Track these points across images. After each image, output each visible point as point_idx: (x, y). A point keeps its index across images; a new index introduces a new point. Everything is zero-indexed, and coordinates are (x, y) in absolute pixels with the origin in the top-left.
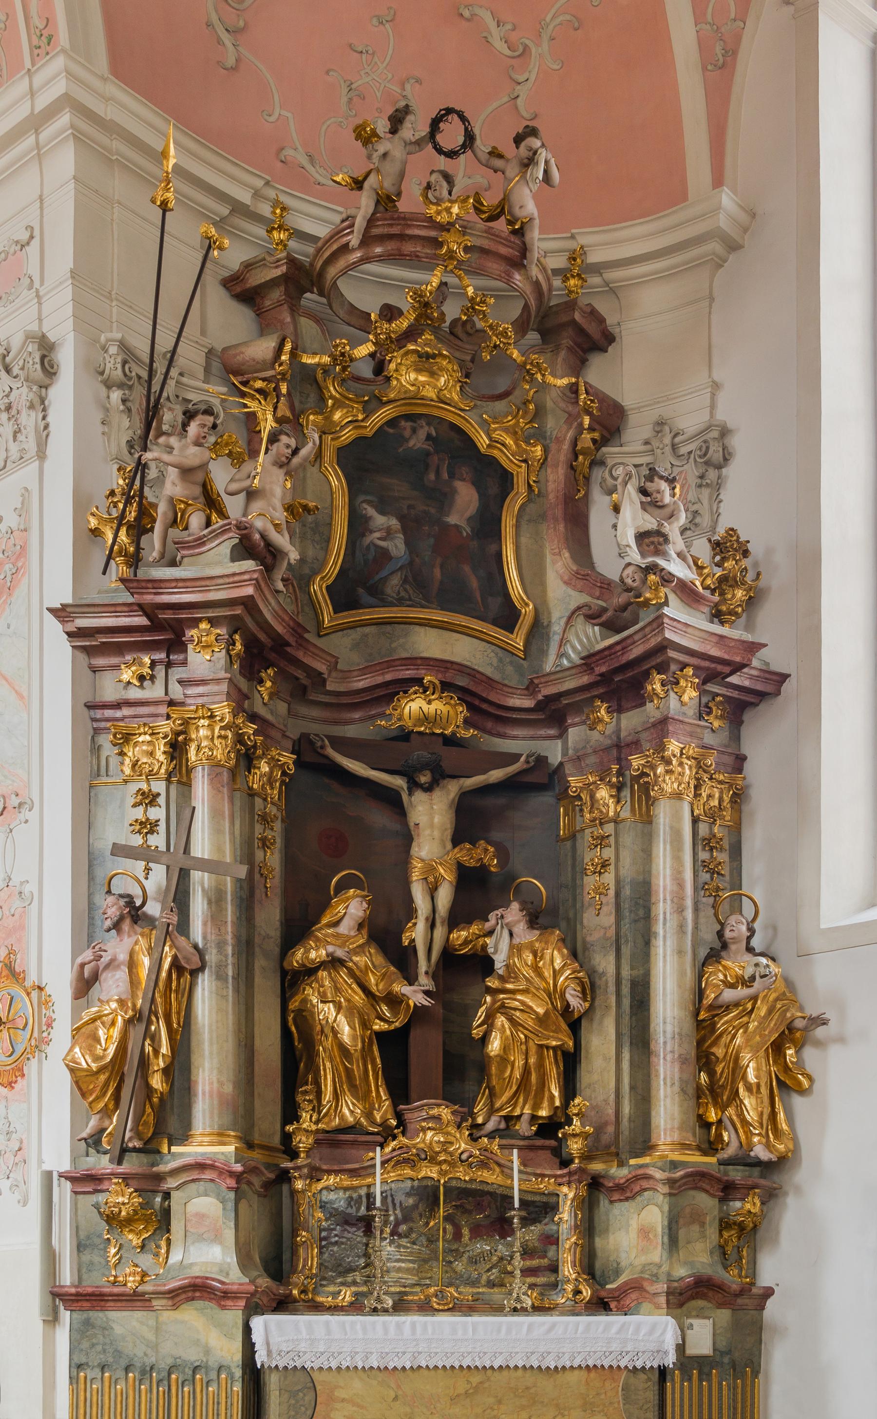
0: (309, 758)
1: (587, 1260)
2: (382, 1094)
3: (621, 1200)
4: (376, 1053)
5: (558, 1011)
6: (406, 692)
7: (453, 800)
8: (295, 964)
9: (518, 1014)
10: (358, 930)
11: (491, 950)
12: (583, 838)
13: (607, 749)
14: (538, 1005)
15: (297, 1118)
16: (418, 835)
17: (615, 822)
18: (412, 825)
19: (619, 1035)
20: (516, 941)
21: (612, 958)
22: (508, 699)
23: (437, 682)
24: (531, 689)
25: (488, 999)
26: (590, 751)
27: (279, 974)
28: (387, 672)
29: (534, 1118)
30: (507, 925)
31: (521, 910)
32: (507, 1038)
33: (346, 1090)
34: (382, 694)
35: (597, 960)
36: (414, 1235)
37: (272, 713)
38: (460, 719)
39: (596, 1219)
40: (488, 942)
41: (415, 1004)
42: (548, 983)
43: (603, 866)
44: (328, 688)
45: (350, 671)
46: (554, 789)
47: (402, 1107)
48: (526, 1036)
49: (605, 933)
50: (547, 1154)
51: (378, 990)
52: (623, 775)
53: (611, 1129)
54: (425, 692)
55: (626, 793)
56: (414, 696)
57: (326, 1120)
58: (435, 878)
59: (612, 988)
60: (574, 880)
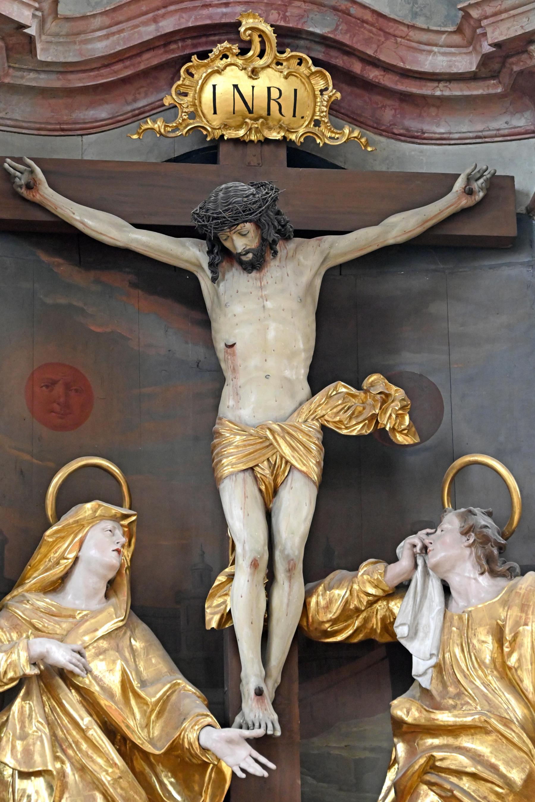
6: (203, 55)
7: (310, 285)
9: (466, 783)
10: (107, 596)
14: (510, 763)
16: (234, 370)
18: (220, 346)
22: (421, 57)
23: (268, 29)
24: (468, 31)
25: (401, 749)
28: (163, 16)
30: (435, 568)
31: (465, 533)
34: (155, 62)
38: (322, 107)
40: (396, 610)
41: (234, 774)
45: (84, 18)
51: (151, 741)
54: (244, 51)
58: (273, 467)
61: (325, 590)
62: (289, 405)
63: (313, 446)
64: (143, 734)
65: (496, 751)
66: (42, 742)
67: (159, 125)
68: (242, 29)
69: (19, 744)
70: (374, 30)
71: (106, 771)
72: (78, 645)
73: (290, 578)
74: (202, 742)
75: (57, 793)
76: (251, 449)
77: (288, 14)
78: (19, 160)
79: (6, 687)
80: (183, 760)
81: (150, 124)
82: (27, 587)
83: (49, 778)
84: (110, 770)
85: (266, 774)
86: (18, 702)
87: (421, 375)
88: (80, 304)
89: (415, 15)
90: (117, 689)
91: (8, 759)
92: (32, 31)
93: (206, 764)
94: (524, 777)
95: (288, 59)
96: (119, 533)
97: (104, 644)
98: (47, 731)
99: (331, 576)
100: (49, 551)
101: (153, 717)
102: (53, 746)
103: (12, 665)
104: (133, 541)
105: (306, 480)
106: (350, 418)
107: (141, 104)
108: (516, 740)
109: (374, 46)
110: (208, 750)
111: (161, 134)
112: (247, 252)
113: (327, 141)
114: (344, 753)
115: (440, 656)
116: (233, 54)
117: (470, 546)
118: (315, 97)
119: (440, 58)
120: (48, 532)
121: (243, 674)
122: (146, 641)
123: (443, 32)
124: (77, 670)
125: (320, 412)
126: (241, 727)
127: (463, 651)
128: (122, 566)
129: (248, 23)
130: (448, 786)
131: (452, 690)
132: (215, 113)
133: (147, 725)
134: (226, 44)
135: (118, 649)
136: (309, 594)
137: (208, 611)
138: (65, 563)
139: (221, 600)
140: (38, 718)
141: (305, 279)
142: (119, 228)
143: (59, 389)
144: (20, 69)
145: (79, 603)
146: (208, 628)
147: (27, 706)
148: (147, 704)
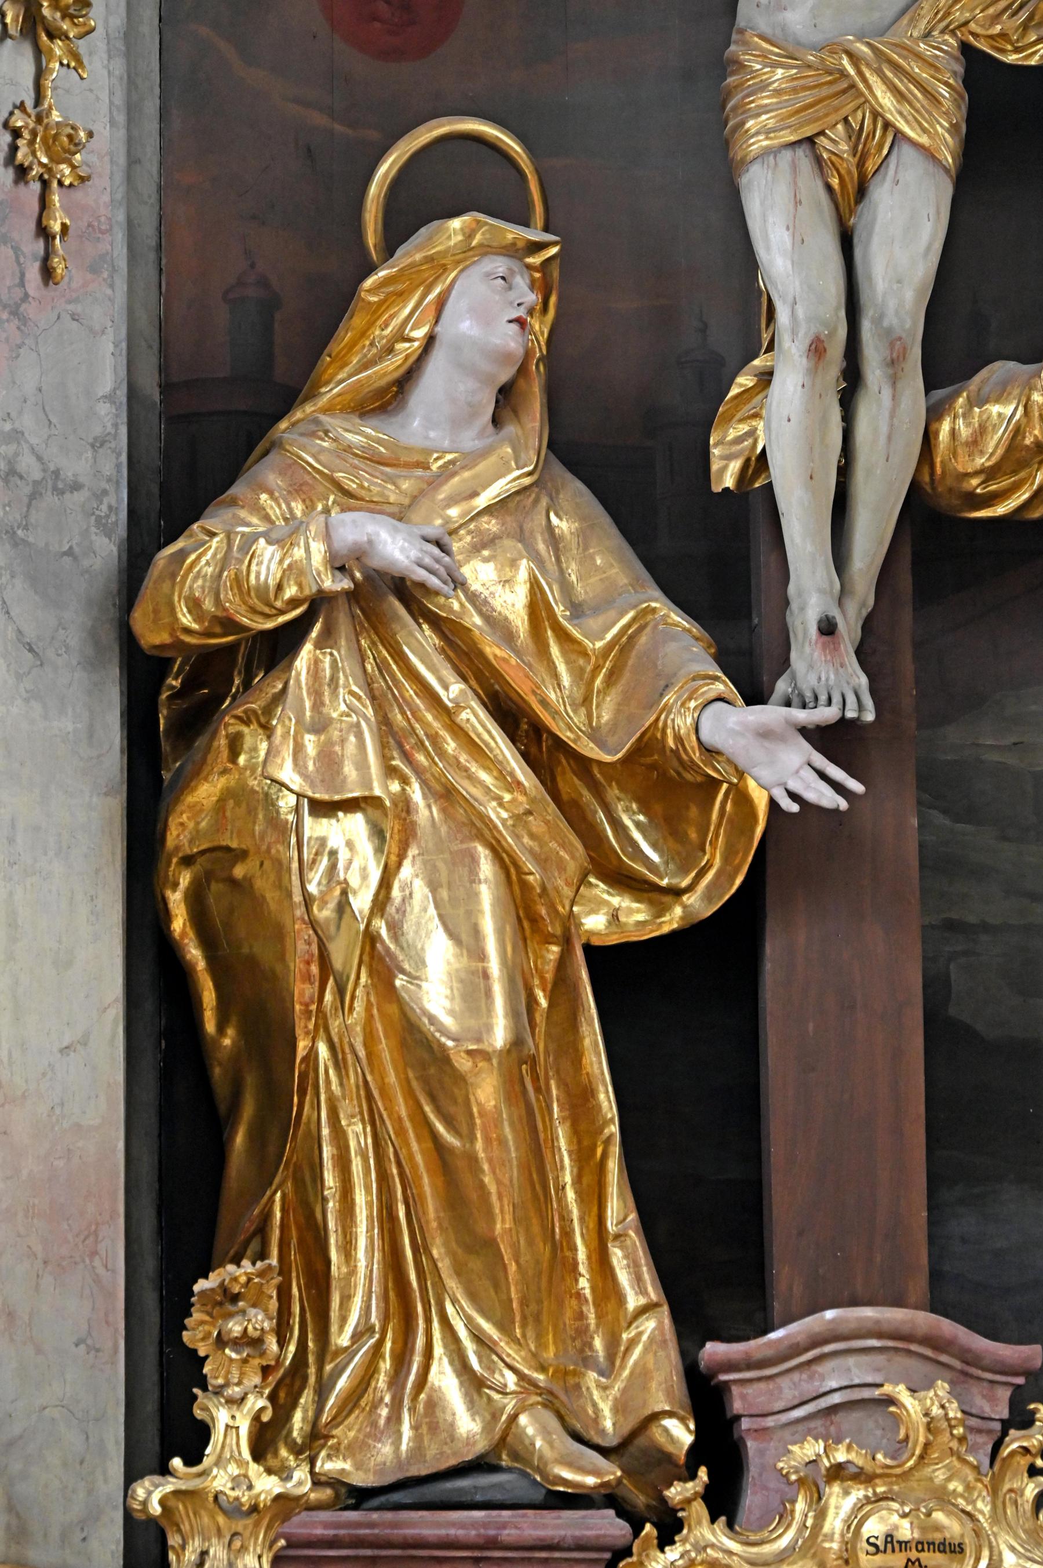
2: (623, 1277)
8: (186, 619)
10: (496, 421)
27: (114, 672)
33: (444, 1266)
41: (773, 804)
47: (714, 1350)
51: (595, 735)
57: (346, 1433)
58: (855, 136)
61: (971, 404)
63: (944, 91)
64: (579, 719)
66: (359, 735)
69: (311, 743)
71: (499, 799)
72: (435, 527)
73: (894, 381)
74: (705, 735)
75: (392, 845)
76: (807, 96)
79: (282, 619)
80: (663, 774)
82: (323, 401)
83: (375, 814)
84: (507, 797)
85: (843, 804)
86: (307, 651)
90: (519, 618)
91: (287, 773)
93: (715, 784)
96: (521, 282)
97: (491, 525)
98: (370, 712)
99: (984, 373)
100: (371, 324)
101: (598, 682)
102: (383, 747)
104: (553, 300)
105: (931, 168)
106: (1025, 27)
110: (719, 753)
114: (1011, 760)
120: (369, 283)
121: (792, 589)
122: (582, 519)
124: (434, 581)
125: (958, 15)
126: (788, 704)
128: (528, 354)
133: (586, 701)
135: (522, 536)
136: (934, 414)
137: (716, 452)
139: (743, 428)
140: (350, 684)
145: (437, 436)
146: (717, 488)
147: (328, 659)
148: (584, 653)
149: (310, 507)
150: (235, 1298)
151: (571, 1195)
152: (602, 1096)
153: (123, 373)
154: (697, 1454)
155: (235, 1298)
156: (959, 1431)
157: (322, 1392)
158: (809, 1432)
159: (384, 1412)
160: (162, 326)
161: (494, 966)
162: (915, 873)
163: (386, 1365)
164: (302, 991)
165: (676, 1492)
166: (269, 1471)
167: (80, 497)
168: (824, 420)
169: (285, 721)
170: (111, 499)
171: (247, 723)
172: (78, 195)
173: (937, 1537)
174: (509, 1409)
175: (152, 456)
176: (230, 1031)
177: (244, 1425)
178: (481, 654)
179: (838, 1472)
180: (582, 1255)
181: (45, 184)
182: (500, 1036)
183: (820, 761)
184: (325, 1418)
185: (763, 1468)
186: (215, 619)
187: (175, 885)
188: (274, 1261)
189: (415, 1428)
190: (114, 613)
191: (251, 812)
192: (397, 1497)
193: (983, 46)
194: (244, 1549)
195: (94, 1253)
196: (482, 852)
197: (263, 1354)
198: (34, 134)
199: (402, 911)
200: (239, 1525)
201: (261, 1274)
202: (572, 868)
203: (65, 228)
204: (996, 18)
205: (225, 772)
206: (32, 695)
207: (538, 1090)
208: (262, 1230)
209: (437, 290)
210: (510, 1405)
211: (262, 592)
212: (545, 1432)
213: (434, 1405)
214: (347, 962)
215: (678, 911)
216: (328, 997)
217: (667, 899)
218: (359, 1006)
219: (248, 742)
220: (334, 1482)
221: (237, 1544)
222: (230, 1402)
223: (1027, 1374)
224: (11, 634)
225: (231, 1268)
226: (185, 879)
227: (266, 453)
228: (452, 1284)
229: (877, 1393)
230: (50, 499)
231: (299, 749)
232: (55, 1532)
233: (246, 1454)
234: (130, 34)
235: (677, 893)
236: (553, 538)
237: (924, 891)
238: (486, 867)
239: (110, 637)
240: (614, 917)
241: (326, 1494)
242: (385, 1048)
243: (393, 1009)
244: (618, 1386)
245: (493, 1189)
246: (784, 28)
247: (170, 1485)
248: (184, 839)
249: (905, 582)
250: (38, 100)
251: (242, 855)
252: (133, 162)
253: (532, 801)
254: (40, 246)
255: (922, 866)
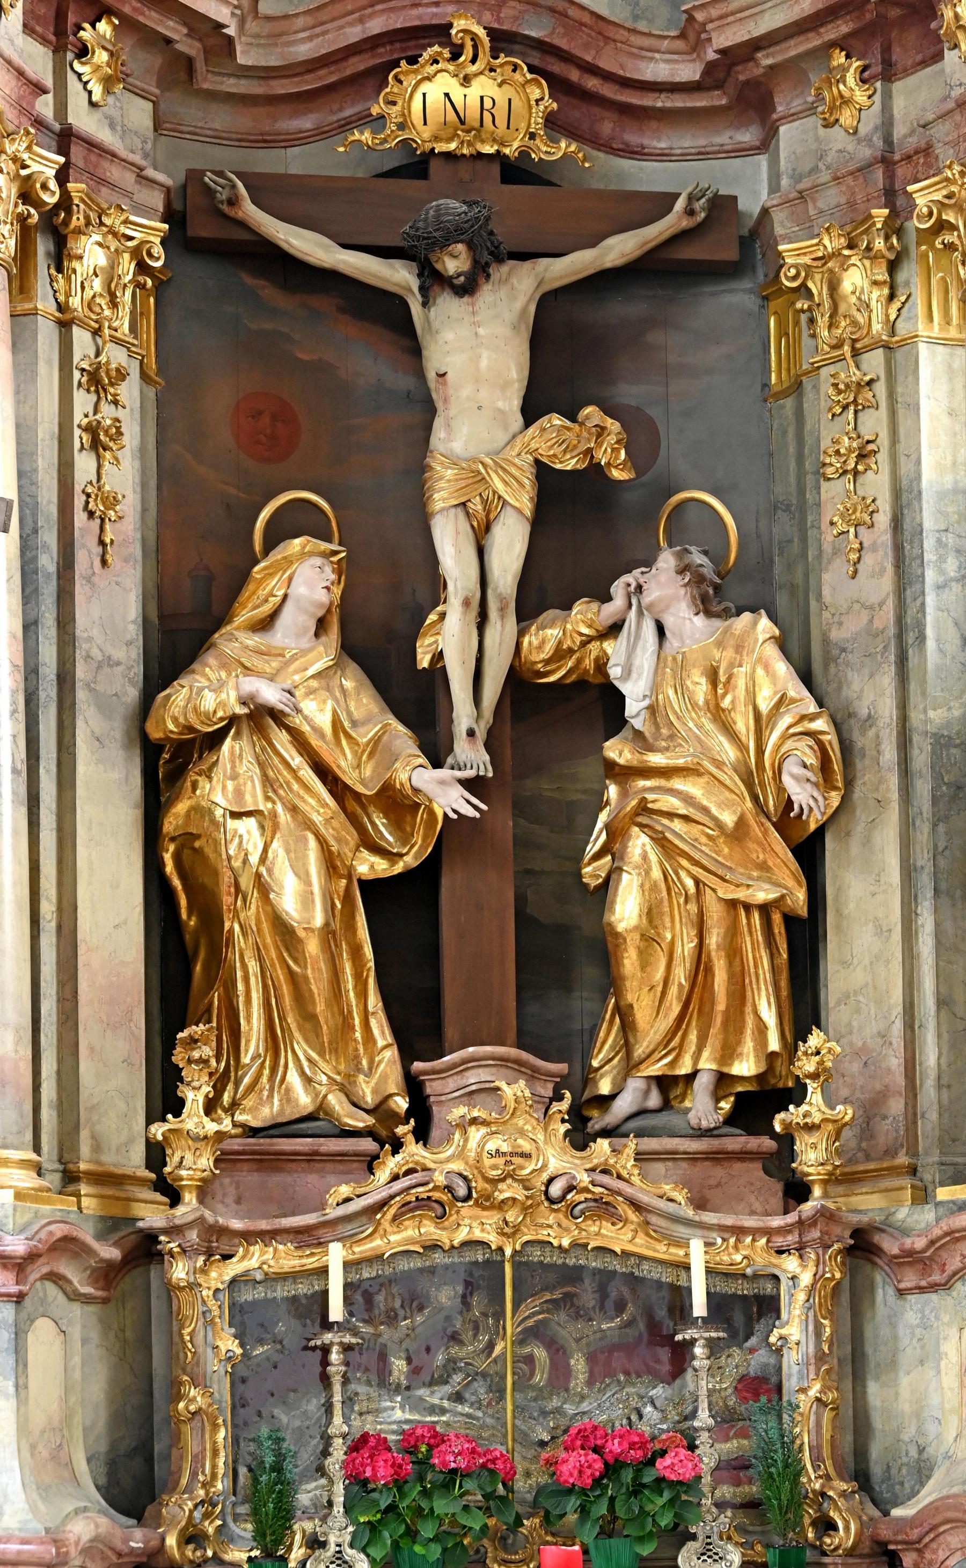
0: (201, 228)
1: (849, 1438)
2: (376, 1032)
3: (921, 1290)
4: (363, 933)
5: (769, 818)
6: (413, 60)
7: (524, 311)
8: (171, 726)
9: (677, 825)
10: (317, 635)
11: (614, 672)
12: (816, 388)
13: (863, 170)
15: (176, 1106)
16: (446, 401)
17: (887, 347)
18: (431, 375)
19: (908, 871)
20: (672, 643)
21: (887, 680)
22: (642, 65)
23: (481, 32)
24: (692, 36)
25: (613, 791)
26: (825, 177)
27: (137, 751)
28: (370, 16)
29: (723, 1080)
30: (650, 607)
31: (681, 572)
32: (654, 887)
33: (293, 1026)
34: (362, 67)
35: (856, 686)
36: (457, 1378)
37: (112, 126)
39: (868, 1333)
40: (609, 651)
41: (445, 815)
42: (741, 747)
43: (862, 456)
44: (241, 59)
45: (286, 17)
46: (754, 271)
47: (418, 1066)
48: (697, 882)
49: (871, 621)
50: (756, 1169)
51: (363, 782)
52: (900, 232)
53: (896, 1106)
54: (455, 56)
55: (910, 273)
56: (432, 69)
57: (248, 1103)
58: (485, 502)
59: (889, 754)
60: (801, 491)
61: (538, 629)
62: (502, 438)
63: (527, 481)
64: (355, 774)
65: (708, 792)
66: (253, 781)
67: (366, 137)
68: (453, 32)
69: (230, 785)
70: (593, 34)
71: (318, 812)
72: (288, 684)
73: (502, 618)
74: (414, 783)
75: (268, 833)
77: (502, 15)
78: (220, 174)
79: (216, 727)
80: (394, 801)
81: (357, 135)
82: (235, 624)
83: (261, 818)
86: (228, 742)
87: (638, 408)
88: (286, 330)
89: (636, 18)
90: (328, 729)
91: (218, 798)
92: (231, 31)
93: (419, 805)
94: (735, 819)
95: (502, 65)
96: (328, 569)
97: (314, 684)
98: (258, 771)
99: (545, 615)
100: (257, 588)
101: (364, 758)
102: (264, 786)
103: (222, 704)
104: (343, 578)
105: (520, 517)
106: (565, 451)
107: (347, 113)
108: (728, 782)
109: (593, 52)
111: (369, 147)
112: (459, 275)
113: (543, 156)
114: (556, 795)
115: (654, 698)
116: (444, 59)
117: (685, 585)
118: (530, 107)
119: (662, 66)
121: (454, 715)
122: (357, 681)
123: (666, 37)
124: (287, 710)
125: (533, 445)
126: (453, 768)
127: (676, 692)
128: (331, 603)
129: (460, 24)
130: (659, 828)
131: (664, 731)
132: (425, 124)
133: (359, 766)
134: (436, 48)
135: (328, 689)
136: (521, 633)
137: (419, 650)
138: (274, 601)
139: (432, 639)
140: (248, 757)
141: (519, 304)
142: (326, 249)
143: (266, 420)
144: (220, 74)
145: (290, 642)
146: (420, 667)
147: (237, 746)
148: (358, 744)
149: (229, 674)
150: (196, 1041)
151: (352, 994)
152: (366, 949)
153: (140, 611)
154: (410, 1113)
155: (196, 1041)
156: (530, 1102)
157: (237, 1084)
158: (461, 1103)
159: (266, 1093)
160: (159, 588)
161: (316, 889)
162: (511, 848)
163: (266, 1072)
164: (227, 900)
165: (400, 1130)
166: (213, 1120)
167: (120, 669)
168: (470, 637)
169: (218, 774)
170: (135, 670)
171: (200, 775)
172: (117, 525)
173: (520, 1150)
174: (323, 1092)
175: (156, 651)
176: (194, 918)
177: (201, 1099)
178: (309, 744)
179: (474, 1121)
180: (357, 1021)
181: (102, 520)
182: (318, 920)
183: (468, 795)
184: (238, 1096)
185: (440, 1119)
186: (185, 727)
187: (167, 851)
188: (214, 1024)
189: (280, 1100)
190: (137, 723)
191: (203, 817)
192: (272, 1132)
193: (545, 460)
194: (200, 1155)
195: (130, 1020)
196: (311, 838)
197: (209, 1067)
198: (97, 496)
199: (273, 863)
200: (198, 1145)
201: (208, 1030)
202: (352, 844)
203: (112, 541)
204: (551, 447)
205: (190, 798)
206: (98, 761)
207: (336, 946)
208: (209, 1010)
209: (288, 573)
210: (324, 1090)
211: (207, 714)
212: (341, 1103)
213: (288, 1090)
214: (248, 886)
215: (401, 864)
216: (239, 903)
217: (396, 858)
218: (253, 907)
219: (201, 784)
220: (243, 1126)
221: (198, 1153)
222: (194, 1088)
223: (561, 1076)
224: (89, 733)
225: (194, 1027)
226: (172, 848)
227: (208, 649)
228: (297, 1034)
229: (492, 1085)
230: (106, 670)
231: (224, 787)
232: (114, 1148)
233: (202, 1113)
234: (142, 450)
235: (401, 855)
236: (343, 691)
237: (515, 855)
238: (312, 843)
239: (135, 734)
240: (372, 867)
241: (239, 1130)
242: (265, 927)
243: (269, 909)
244: (374, 1081)
245: (316, 991)
246: (451, 450)
247: (166, 1127)
248: (171, 828)
249: (507, 711)
250: (99, 480)
251: (198, 837)
252: (144, 510)
253: (334, 812)
254: (100, 549)
255: (515, 844)
